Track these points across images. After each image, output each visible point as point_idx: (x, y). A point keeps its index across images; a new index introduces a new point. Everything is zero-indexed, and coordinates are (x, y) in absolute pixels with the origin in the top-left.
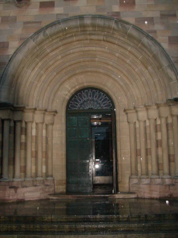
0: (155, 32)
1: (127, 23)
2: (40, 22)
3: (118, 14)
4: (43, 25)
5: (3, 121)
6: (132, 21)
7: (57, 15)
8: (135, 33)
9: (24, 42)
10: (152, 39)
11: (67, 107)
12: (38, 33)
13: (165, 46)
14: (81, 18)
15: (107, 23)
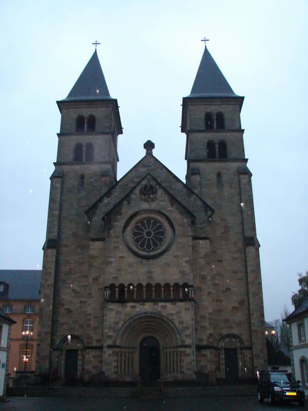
0: (173, 319)
1: (164, 316)
2: (131, 314)
3: (160, 312)
4: (132, 316)
5: (118, 352)
6: (165, 315)
7: (137, 311)
8: (166, 320)
9: (125, 323)
10: (172, 322)
11: (140, 345)
12: (130, 318)
13: (177, 325)
14: (146, 313)
15: (155, 315)
